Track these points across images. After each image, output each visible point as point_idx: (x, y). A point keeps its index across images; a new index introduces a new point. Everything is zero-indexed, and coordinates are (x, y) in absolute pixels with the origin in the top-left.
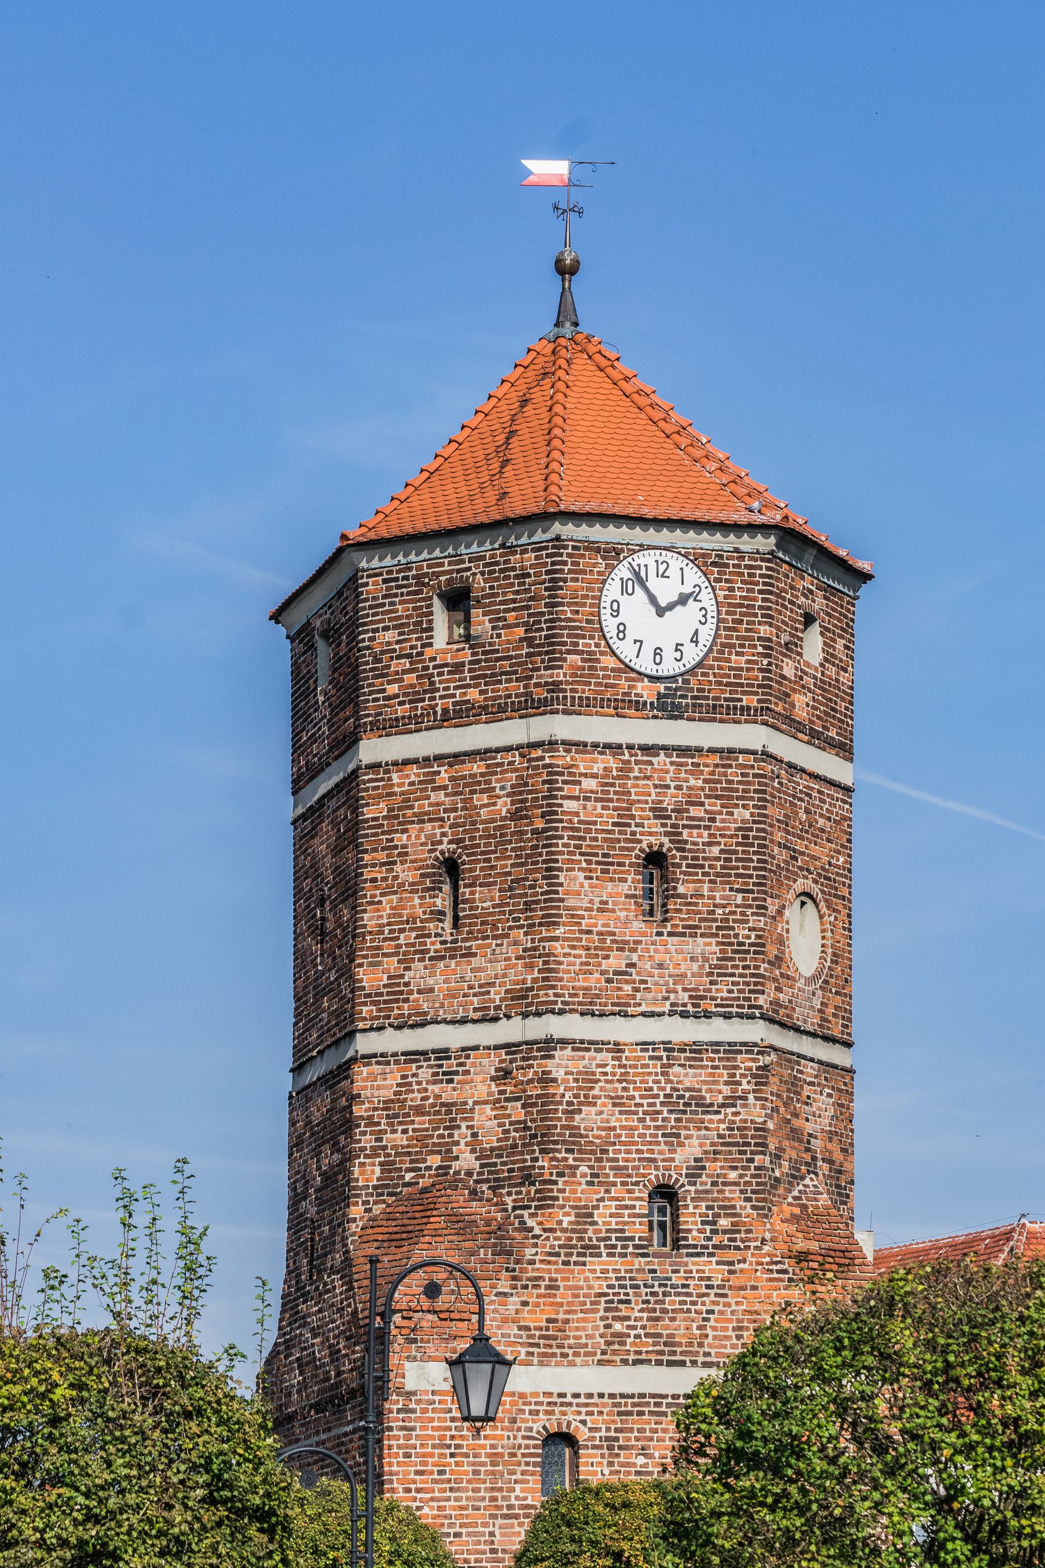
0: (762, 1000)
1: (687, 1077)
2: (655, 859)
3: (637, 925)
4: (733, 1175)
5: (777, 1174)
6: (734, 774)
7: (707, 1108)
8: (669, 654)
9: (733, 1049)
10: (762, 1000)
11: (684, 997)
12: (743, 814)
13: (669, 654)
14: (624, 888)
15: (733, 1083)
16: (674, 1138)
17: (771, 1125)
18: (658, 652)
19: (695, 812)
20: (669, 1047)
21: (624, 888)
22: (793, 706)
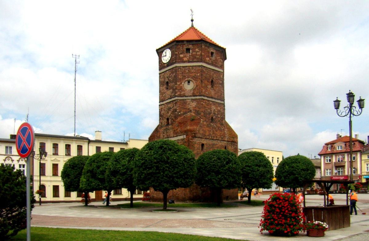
0: (176, 94)
1: (169, 105)
2: (167, 83)
3: (166, 90)
4: (173, 115)
5: (180, 114)
6: (174, 70)
7: (171, 108)
8: (167, 60)
9: (173, 101)
10: (176, 94)
11: (169, 97)
12: (174, 74)
13: (167, 60)
14: (164, 87)
15: (173, 105)
16: (168, 113)
17: (178, 108)
18: (166, 60)
19: (170, 76)
20: (168, 103)
21: (164, 87)
22: (183, 59)
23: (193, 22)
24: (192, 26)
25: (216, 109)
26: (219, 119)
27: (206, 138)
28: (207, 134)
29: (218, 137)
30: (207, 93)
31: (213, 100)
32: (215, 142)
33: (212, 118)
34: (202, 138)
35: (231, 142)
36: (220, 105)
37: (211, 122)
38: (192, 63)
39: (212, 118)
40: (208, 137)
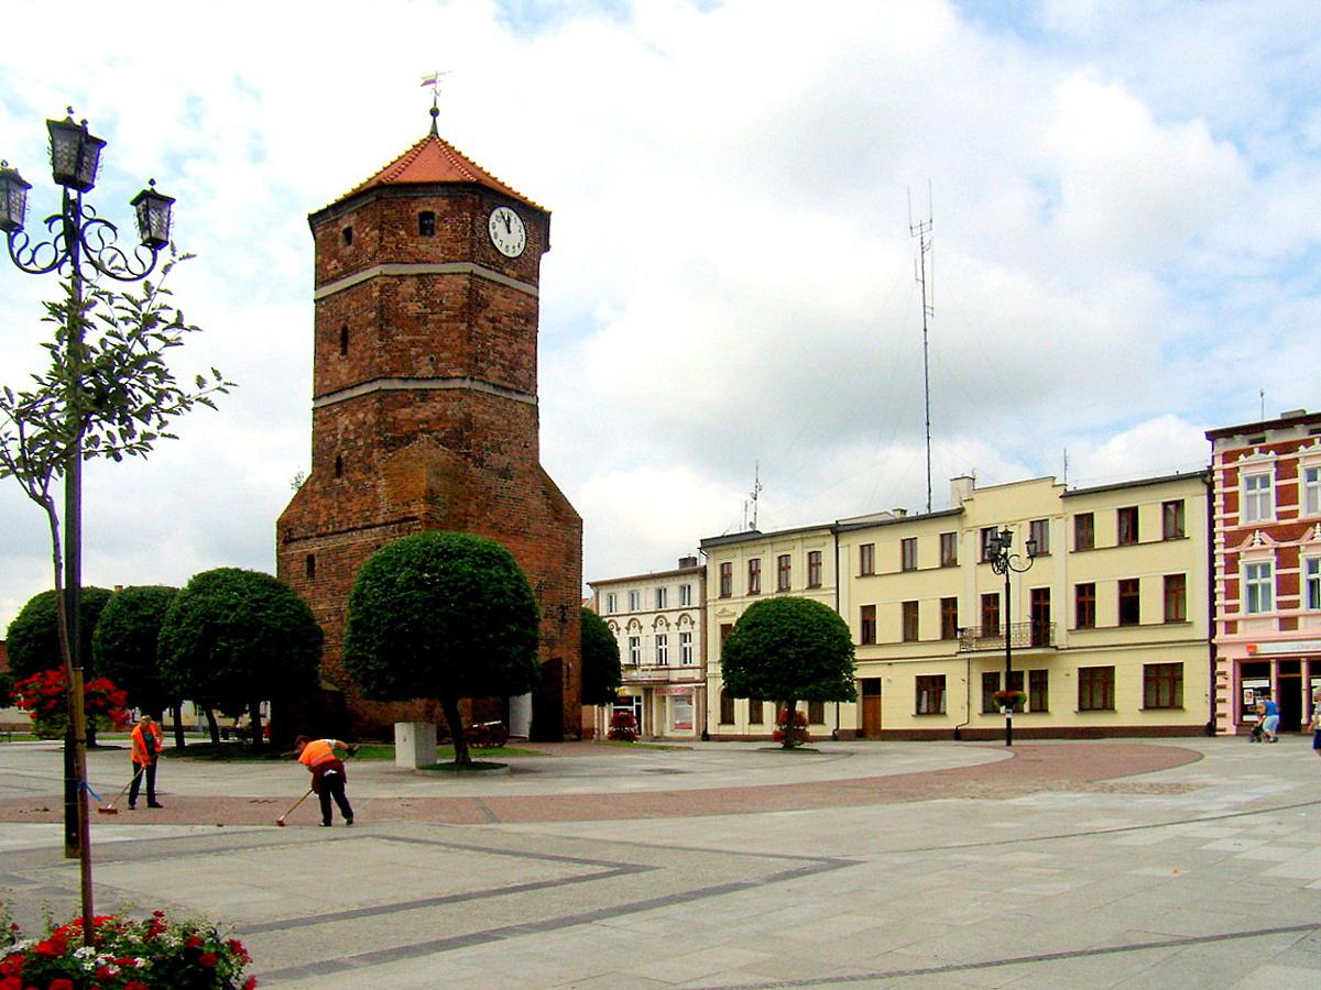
23: (437, 118)
24: (434, 131)
25: (351, 421)
26: (360, 454)
27: (319, 536)
28: (323, 517)
29: (354, 518)
30: (327, 383)
31: (348, 394)
32: (342, 540)
33: (339, 459)
34: (307, 538)
35: (399, 522)
36: (365, 400)
37: (339, 474)
38: (430, 268)
39: (339, 459)
40: (324, 529)
